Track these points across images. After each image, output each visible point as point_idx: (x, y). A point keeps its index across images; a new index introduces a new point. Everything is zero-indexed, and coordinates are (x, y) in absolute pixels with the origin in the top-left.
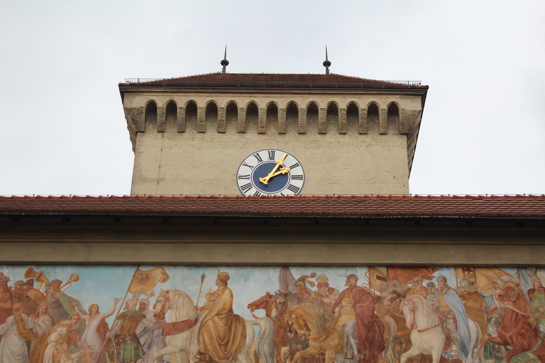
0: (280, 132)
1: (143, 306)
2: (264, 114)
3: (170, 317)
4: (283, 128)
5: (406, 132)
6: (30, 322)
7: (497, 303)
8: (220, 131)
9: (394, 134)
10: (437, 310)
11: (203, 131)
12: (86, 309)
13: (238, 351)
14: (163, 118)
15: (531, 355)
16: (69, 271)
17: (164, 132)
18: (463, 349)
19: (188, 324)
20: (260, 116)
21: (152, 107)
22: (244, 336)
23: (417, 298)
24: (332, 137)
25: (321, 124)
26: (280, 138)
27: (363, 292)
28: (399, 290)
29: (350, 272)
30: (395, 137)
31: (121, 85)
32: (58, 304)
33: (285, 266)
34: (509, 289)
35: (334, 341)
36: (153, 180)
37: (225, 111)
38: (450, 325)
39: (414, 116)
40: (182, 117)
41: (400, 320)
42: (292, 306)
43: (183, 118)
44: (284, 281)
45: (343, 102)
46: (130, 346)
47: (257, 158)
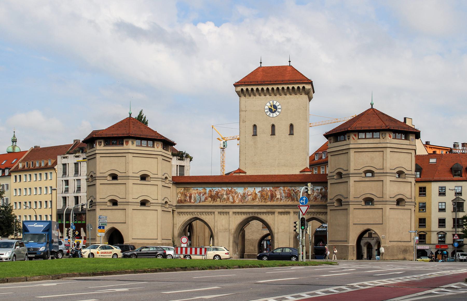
1: (245, 192)
3: (249, 194)
6: (232, 194)
7: (287, 191)
9: (304, 94)
10: (280, 192)
12: (239, 193)
13: (257, 198)
15: (290, 198)
16: (236, 188)
18: (283, 197)
19: (251, 195)
21: (242, 90)
22: (257, 196)
23: (278, 191)
24: (288, 96)
26: (275, 97)
27: (271, 190)
28: (276, 190)
29: (270, 188)
30: (304, 95)
32: (235, 192)
33: (262, 187)
34: (289, 189)
35: (268, 197)
36: (244, 111)
38: (281, 194)
41: (275, 194)
42: (263, 192)
44: (262, 189)
45: (291, 87)
46: (244, 198)
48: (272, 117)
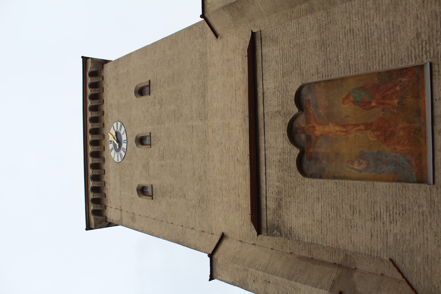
0: (103, 138)
2: (94, 147)
4: (101, 136)
5: (101, 65)
8: (104, 173)
11: (104, 183)
14: (98, 206)
17: (106, 206)
20: (95, 150)
25: (98, 114)
31: (87, 229)
36: (121, 213)
37: (94, 170)
39: (94, 62)
40: (97, 195)
43: (98, 195)
47: (112, 151)
48: (126, 144)
